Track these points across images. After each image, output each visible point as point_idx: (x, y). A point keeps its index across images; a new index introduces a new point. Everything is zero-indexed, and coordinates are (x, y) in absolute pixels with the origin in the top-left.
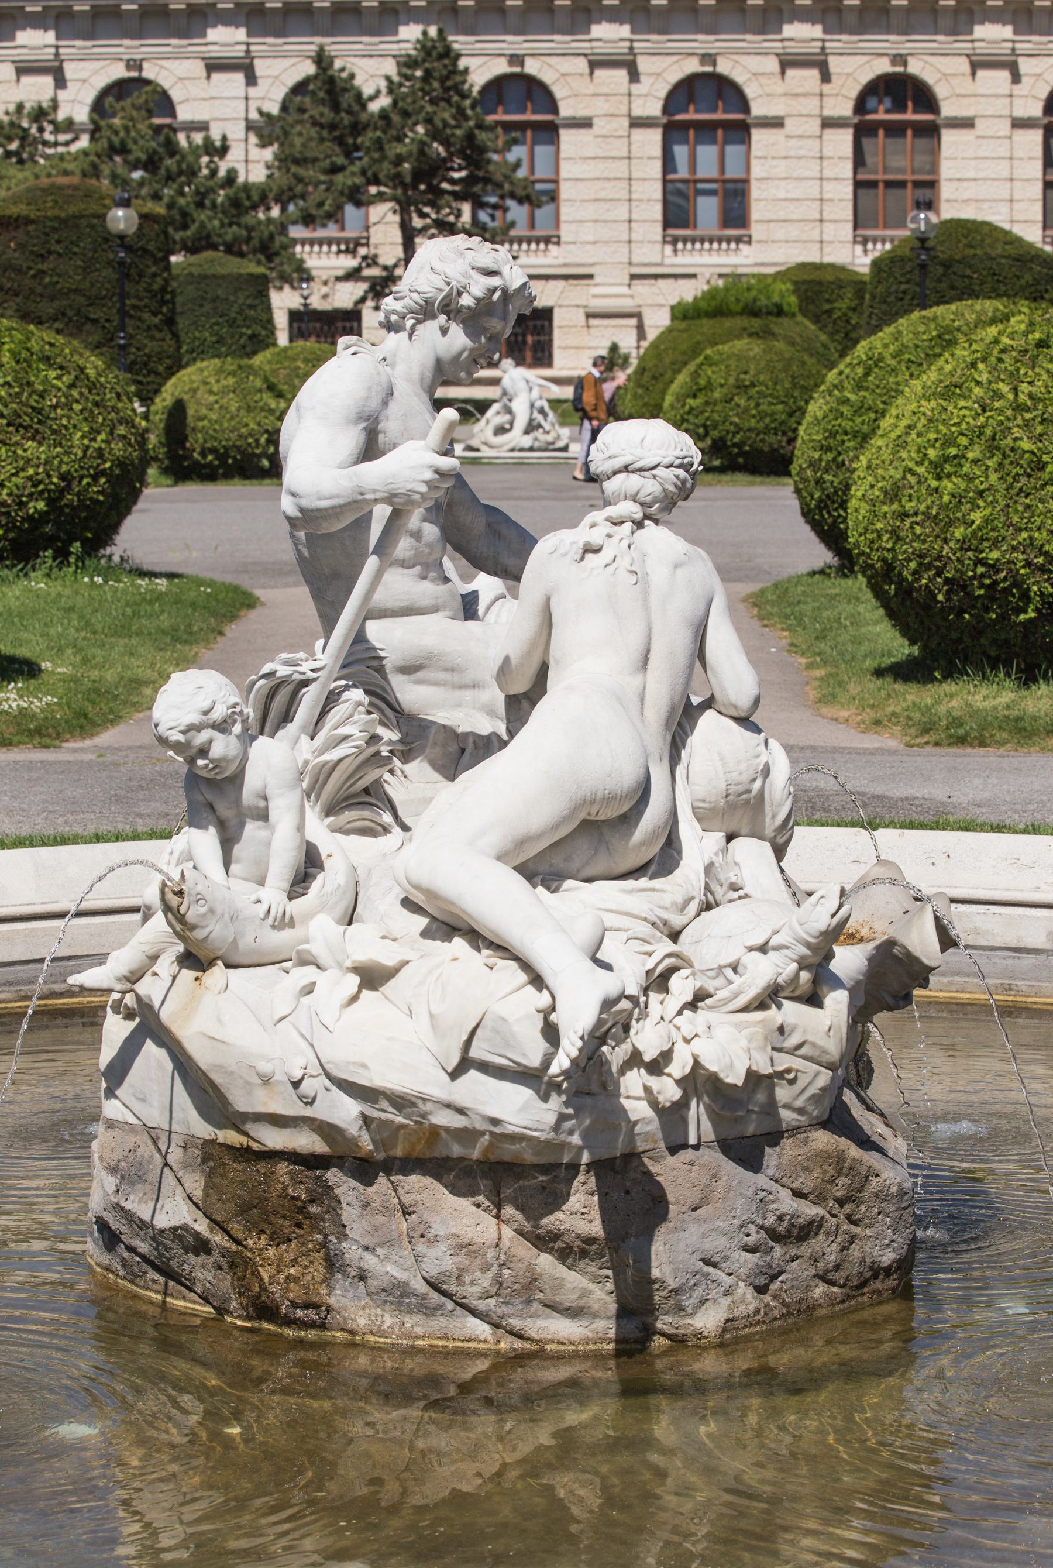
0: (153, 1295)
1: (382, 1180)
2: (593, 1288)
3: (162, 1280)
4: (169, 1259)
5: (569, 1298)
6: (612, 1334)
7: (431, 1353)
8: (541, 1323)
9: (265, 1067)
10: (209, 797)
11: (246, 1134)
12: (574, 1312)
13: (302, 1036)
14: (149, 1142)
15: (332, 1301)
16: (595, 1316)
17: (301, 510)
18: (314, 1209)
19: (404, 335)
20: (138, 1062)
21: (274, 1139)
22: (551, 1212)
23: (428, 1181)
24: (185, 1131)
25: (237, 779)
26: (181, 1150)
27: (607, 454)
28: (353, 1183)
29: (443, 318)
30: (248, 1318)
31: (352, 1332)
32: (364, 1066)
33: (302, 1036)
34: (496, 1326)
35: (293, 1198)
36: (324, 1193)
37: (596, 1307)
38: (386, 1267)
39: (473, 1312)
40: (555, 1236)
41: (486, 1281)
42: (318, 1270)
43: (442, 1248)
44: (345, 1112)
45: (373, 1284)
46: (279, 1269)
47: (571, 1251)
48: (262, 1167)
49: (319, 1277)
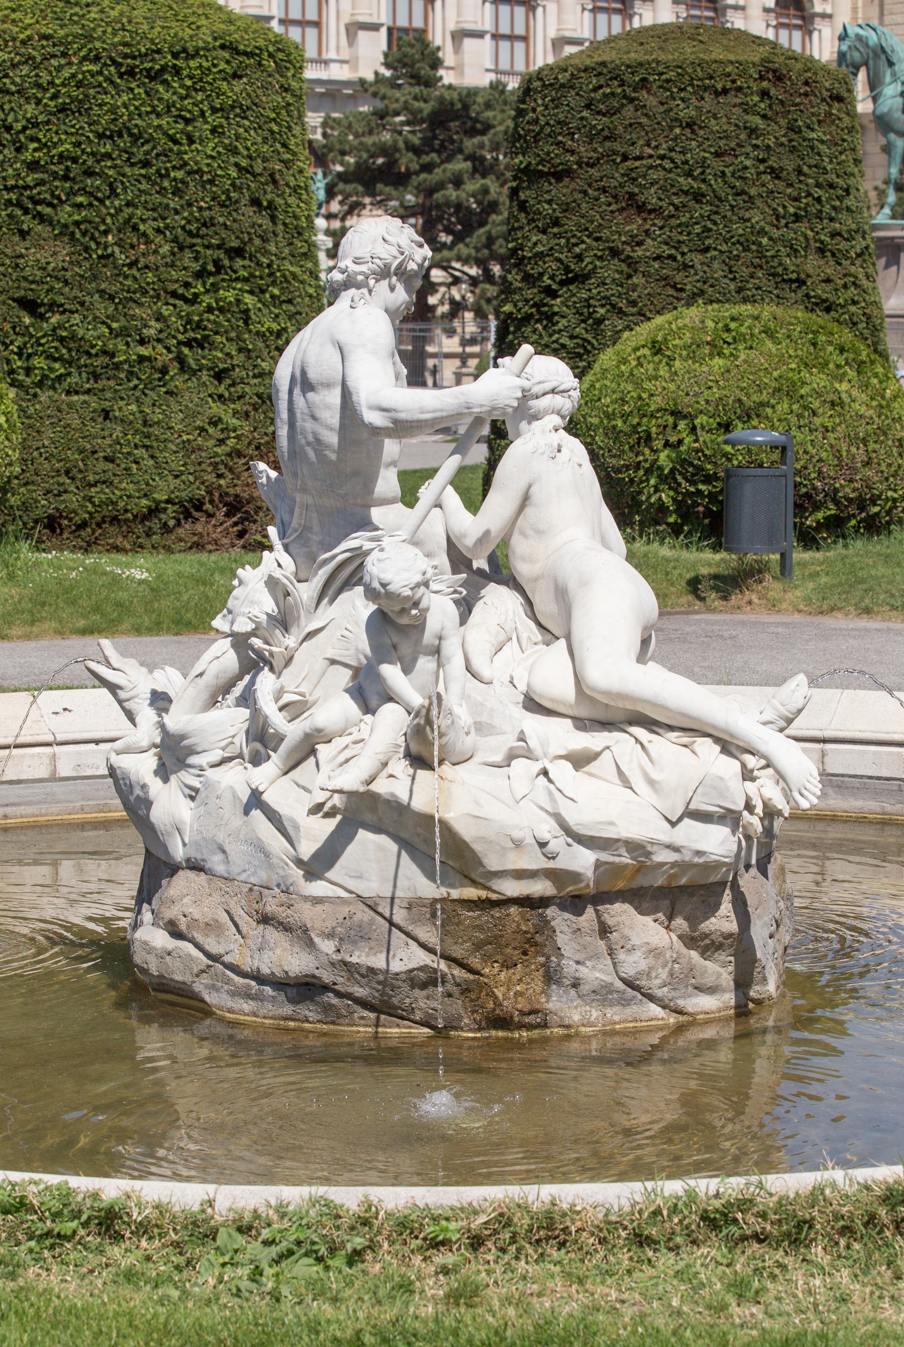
0: (361, 1029)
1: (590, 911)
2: (719, 970)
3: (372, 1015)
4: (391, 997)
5: (709, 981)
6: (733, 1003)
7: (624, 1033)
8: (694, 1000)
9: (517, 834)
10: (395, 639)
11: (489, 889)
12: (712, 990)
13: (541, 808)
14: (366, 909)
15: (550, 1006)
16: (724, 991)
17: (396, 422)
18: (538, 938)
19: (365, 291)
20: (351, 849)
21: (512, 888)
22: (708, 919)
23: (627, 906)
24: (410, 895)
25: (420, 626)
26: (404, 911)
27: (534, 381)
28: (567, 915)
29: (394, 279)
30: (480, 1029)
31: (568, 1027)
32: (611, 823)
33: (541, 808)
34: (664, 1007)
35: (526, 932)
36: (545, 926)
37: (724, 984)
38: (597, 973)
39: (651, 998)
40: (706, 936)
41: (664, 974)
42: (538, 984)
43: (638, 955)
44: (583, 861)
45: (585, 988)
46: (511, 988)
47: (707, 946)
48: (496, 912)
49: (538, 989)
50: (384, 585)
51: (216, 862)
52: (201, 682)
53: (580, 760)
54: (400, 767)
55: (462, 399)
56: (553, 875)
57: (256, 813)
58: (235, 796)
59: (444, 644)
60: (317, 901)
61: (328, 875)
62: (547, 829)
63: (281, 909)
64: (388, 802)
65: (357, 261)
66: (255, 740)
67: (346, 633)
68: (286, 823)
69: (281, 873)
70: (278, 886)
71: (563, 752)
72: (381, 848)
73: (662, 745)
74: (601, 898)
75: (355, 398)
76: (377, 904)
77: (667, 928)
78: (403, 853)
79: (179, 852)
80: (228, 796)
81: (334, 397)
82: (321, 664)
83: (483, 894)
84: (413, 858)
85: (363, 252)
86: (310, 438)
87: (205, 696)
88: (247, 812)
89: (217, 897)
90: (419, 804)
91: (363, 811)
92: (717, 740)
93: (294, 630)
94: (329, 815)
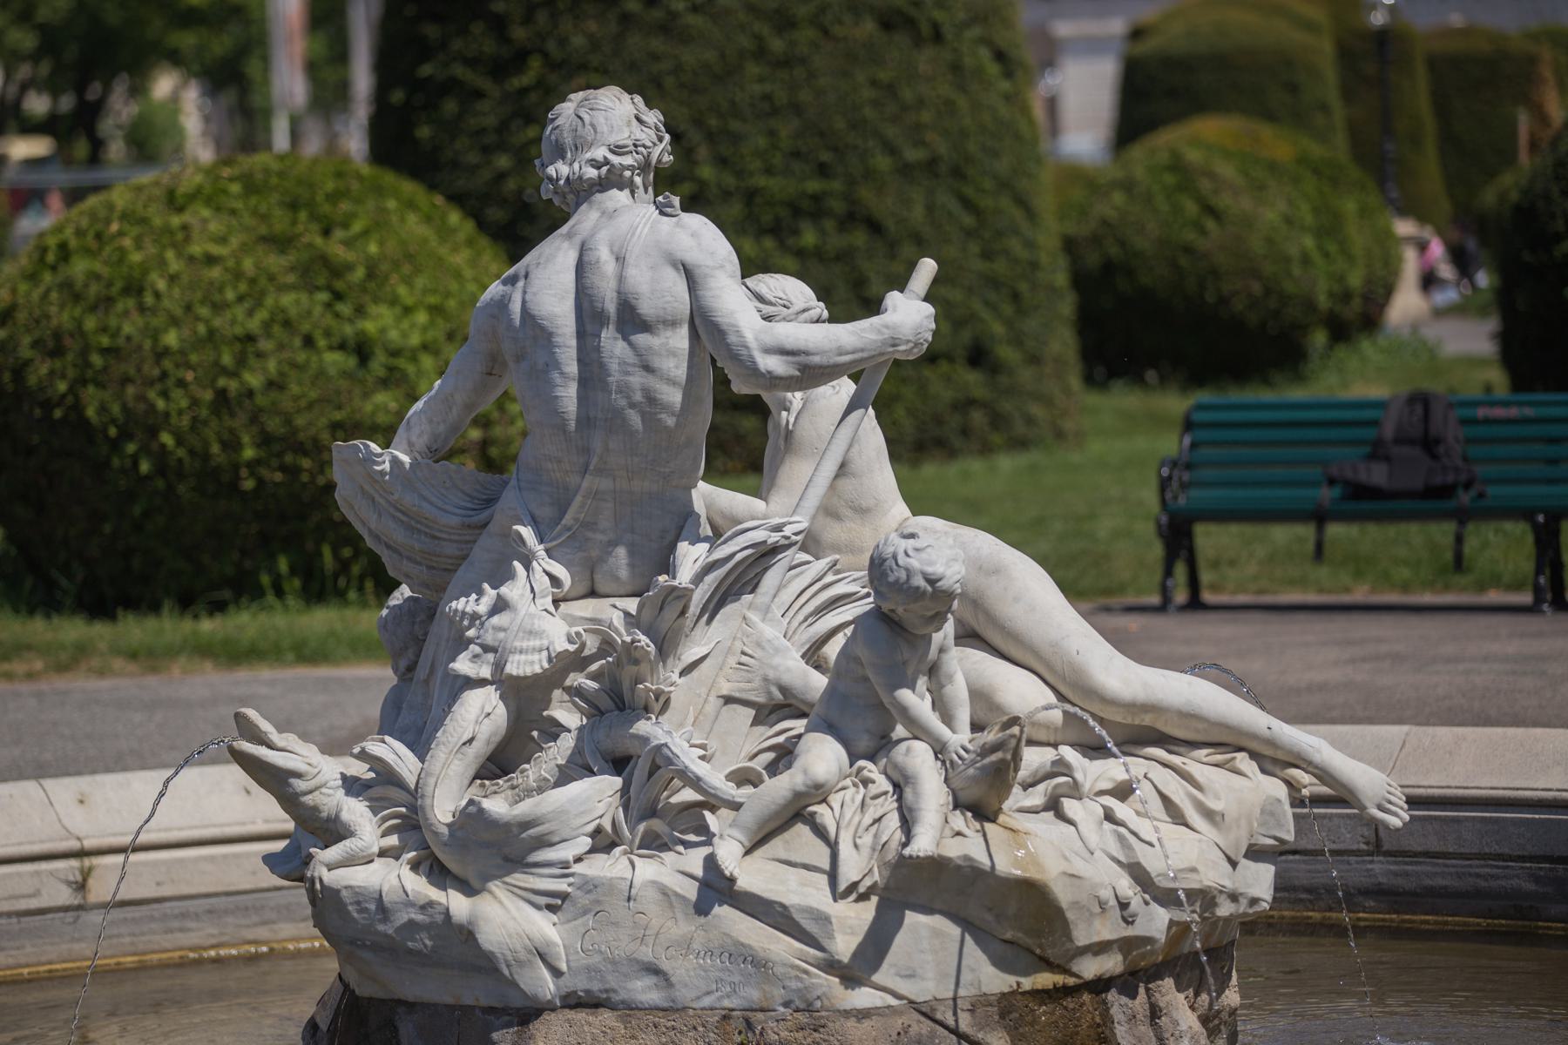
1: (1142, 990)
14: (923, 1019)
17: (804, 368)
20: (900, 940)
21: (1090, 968)
24: (973, 992)
28: (1124, 1000)
32: (1194, 870)
48: (1070, 1003)
50: (932, 581)
51: (643, 990)
52: (471, 751)
53: (1123, 791)
54: (959, 821)
55: (887, 333)
56: (1127, 945)
57: (723, 912)
58: (665, 892)
59: (945, 657)
60: (863, 1014)
61: (877, 978)
62: (1126, 887)
63: (799, 1035)
64: (959, 867)
65: (617, 150)
66: (642, 819)
67: (744, 659)
68: (797, 917)
69: (794, 985)
70: (786, 1004)
71: (1107, 785)
72: (937, 933)
73: (1198, 765)
74: (1154, 973)
75: (732, 339)
76: (933, 1010)
77: (1192, 1008)
78: (968, 937)
79: (545, 985)
80: (652, 894)
81: (680, 340)
82: (714, 703)
83: (1060, 979)
84: (978, 942)
85: (622, 137)
86: (638, 397)
87: (471, 772)
90: (1005, 865)
91: (912, 885)
92: (1254, 755)
93: (670, 661)
94: (863, 897)
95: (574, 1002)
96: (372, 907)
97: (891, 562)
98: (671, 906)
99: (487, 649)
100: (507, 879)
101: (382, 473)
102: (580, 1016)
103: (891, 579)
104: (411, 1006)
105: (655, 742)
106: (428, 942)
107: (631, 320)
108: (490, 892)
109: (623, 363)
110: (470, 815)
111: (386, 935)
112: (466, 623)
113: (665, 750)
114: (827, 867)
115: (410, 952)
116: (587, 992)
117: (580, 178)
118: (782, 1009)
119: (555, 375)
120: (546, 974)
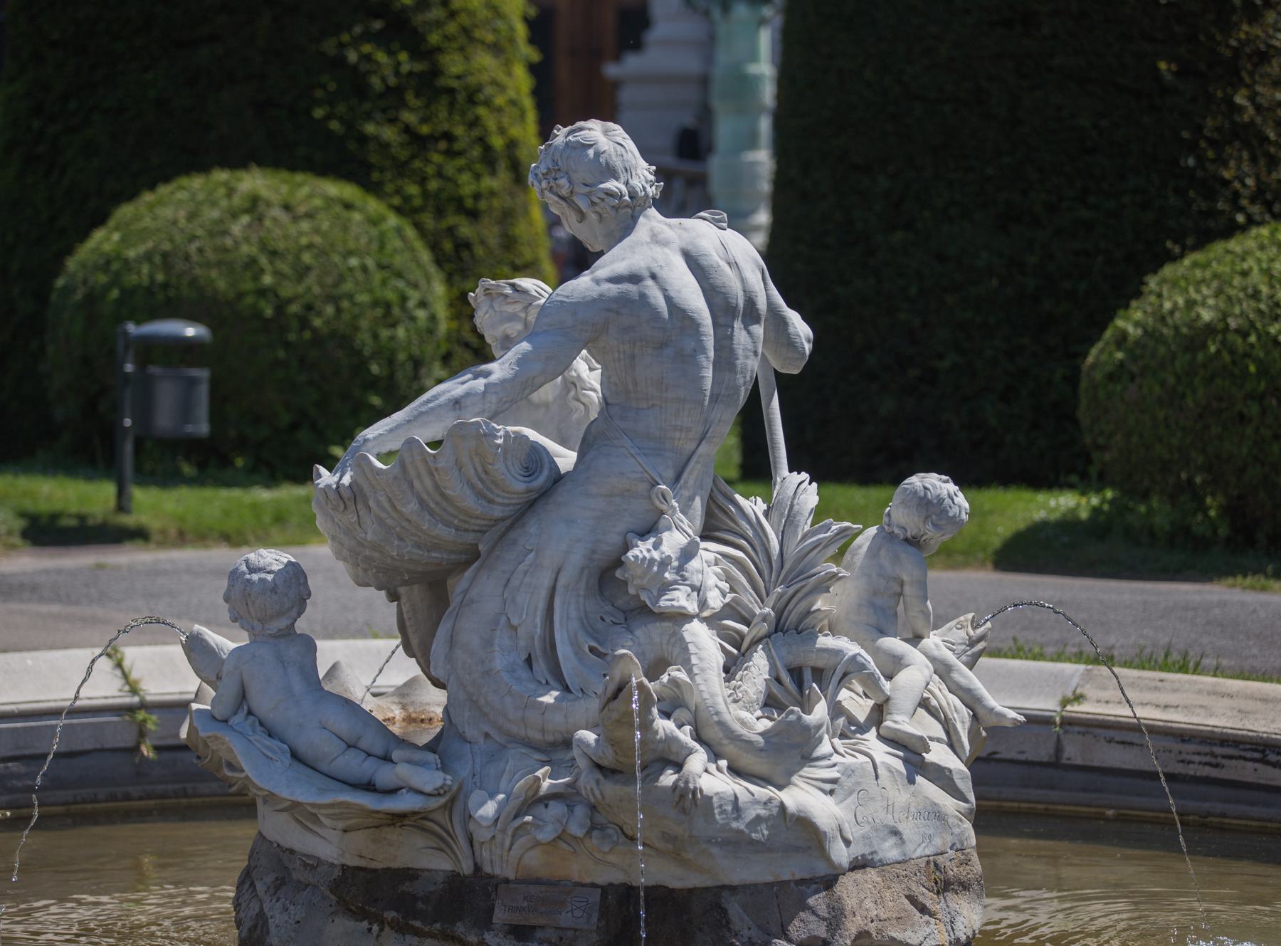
58: (890, 770)
75: (791, 330)
88: (911, 781)
89: (897, 887)
95: (859, 865)
96: (729, 808)
97: (948, 501)
98: (896, 781)
99: (693, 588)
100: (801, 773)
101: (499, 445)
102: (858, 875)
103: (951, 514)
104: (733, 889)
105: (851, 653)
106: (766, 832)
107: (751, 315)
108: (795, 785)
109: (745, 349)
110: (790, 722)
111: (739, 832)
112: (655, 568)
113: (859, 658)
114: (944, 736)
115: (752, 842)
116: (863, 856)
117: (646, 195)
118: (950, 852)
119: (702, 358)
120: (842, 844)
